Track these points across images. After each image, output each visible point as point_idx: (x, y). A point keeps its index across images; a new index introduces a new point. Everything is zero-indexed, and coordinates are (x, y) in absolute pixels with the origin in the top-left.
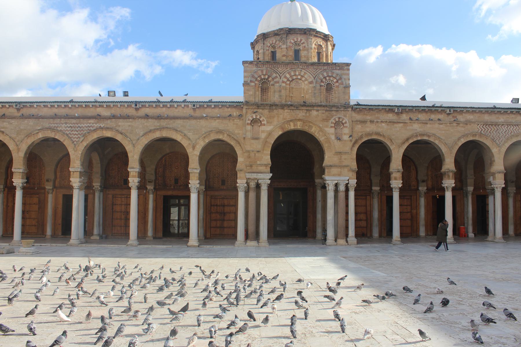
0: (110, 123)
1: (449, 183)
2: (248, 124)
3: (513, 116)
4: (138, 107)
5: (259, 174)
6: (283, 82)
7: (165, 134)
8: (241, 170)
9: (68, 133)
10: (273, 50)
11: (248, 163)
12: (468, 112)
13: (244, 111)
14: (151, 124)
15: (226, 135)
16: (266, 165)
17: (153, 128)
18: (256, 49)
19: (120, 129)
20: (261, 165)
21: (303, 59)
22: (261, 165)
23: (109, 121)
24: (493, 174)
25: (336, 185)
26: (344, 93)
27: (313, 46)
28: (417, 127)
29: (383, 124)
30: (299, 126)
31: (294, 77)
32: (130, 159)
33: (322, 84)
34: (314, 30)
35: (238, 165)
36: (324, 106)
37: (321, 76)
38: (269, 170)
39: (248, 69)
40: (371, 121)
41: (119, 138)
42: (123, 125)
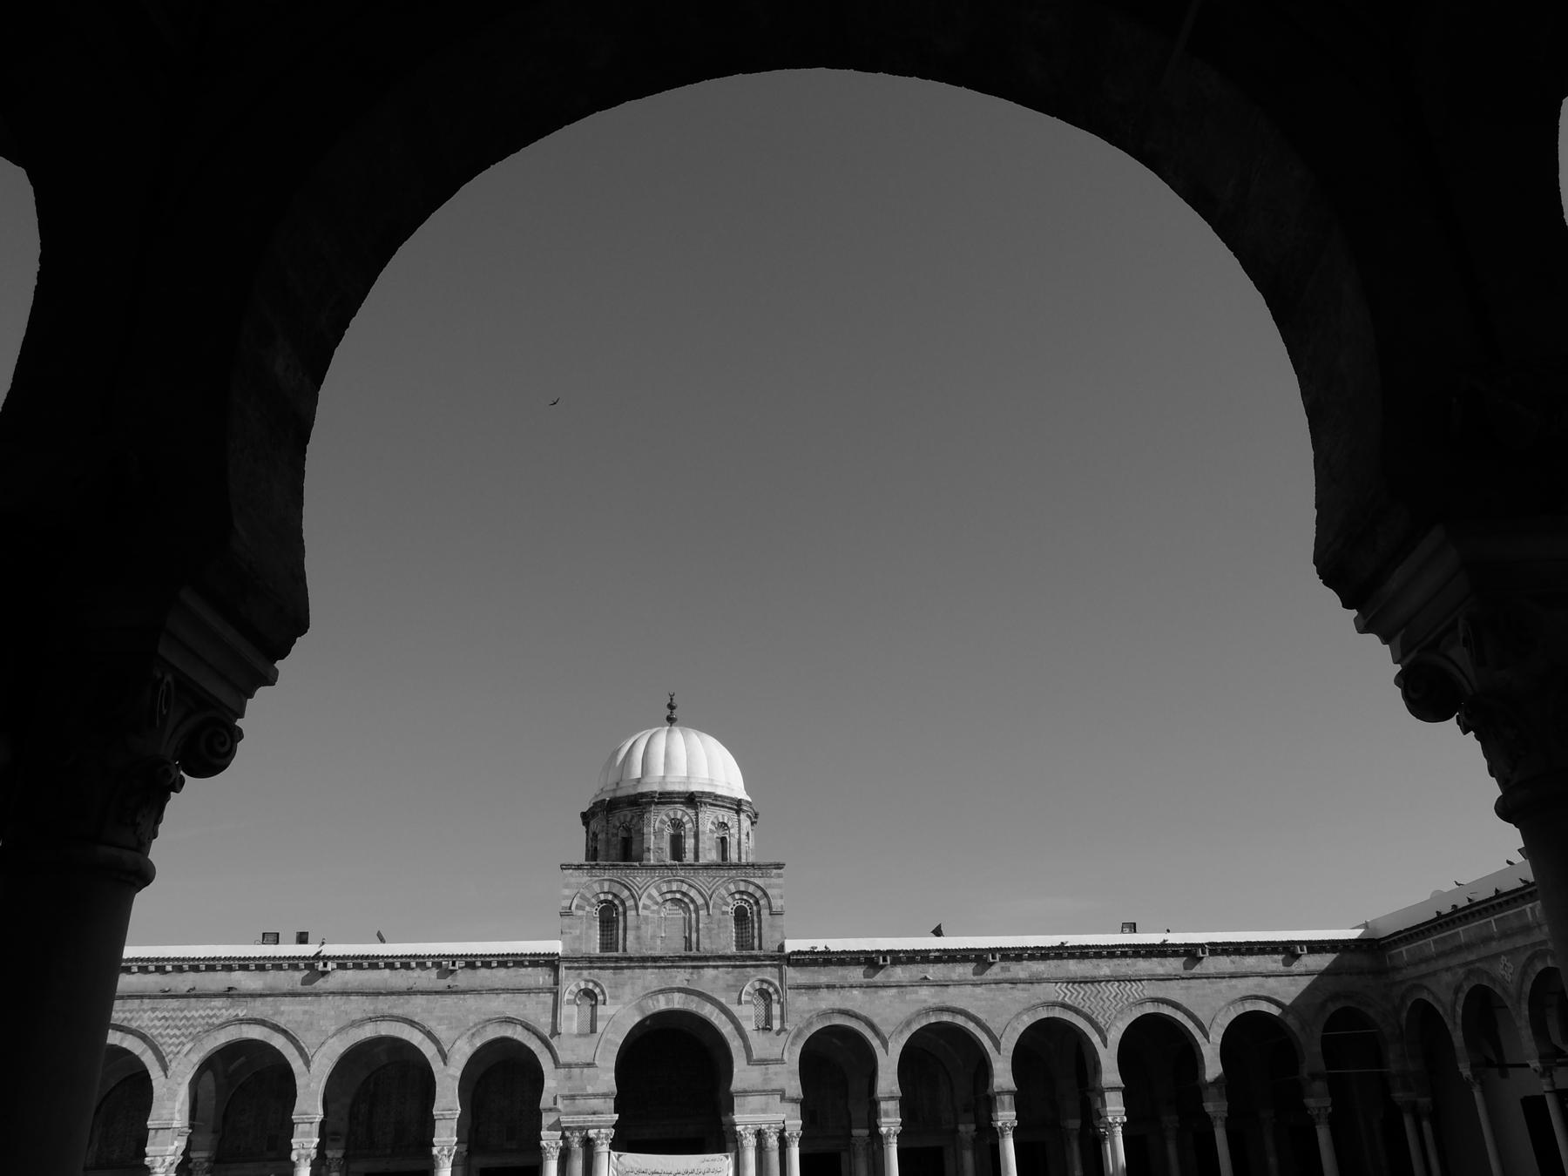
0: (260, 1008)
1: (1006, 1116)
2: (569, 1002)
3: (1128, 961)
4: (329, 968)
5: (590, 1118)
6: (645, 907)
7: (386, 1029)
8: (551, 1110)
9: (156, 1032)
10: (625, 835)
11: (566, 1092)
12: (1032, 958)
13: (563, 972)
14: (358, 1007)
15: (519, 1028)
16: (605, 1096)
17: (358, 1016)
18: (593, 825)
19: (281, 1022)
20: (595, 1096)
21: (689, 857)
22: (595, 1096)
23: (259, 1002)
24: (1101, 1093)
25: (760, 1135)
26: (771, 926)
27: (710, 826)
28: (927, 996)
29: (855, 992)
30: (677, 1002)
31: (669, 896)
32: (299, 1092)
33: (725, 908)
34: (709, 795)
35: (544, 1095)
36: (729, 958)
37: (724, 892)
38: (611, 1104)
39: (573, 880)
40: (828, 987)
41: (278, 1042)
42: (290, 1012)
